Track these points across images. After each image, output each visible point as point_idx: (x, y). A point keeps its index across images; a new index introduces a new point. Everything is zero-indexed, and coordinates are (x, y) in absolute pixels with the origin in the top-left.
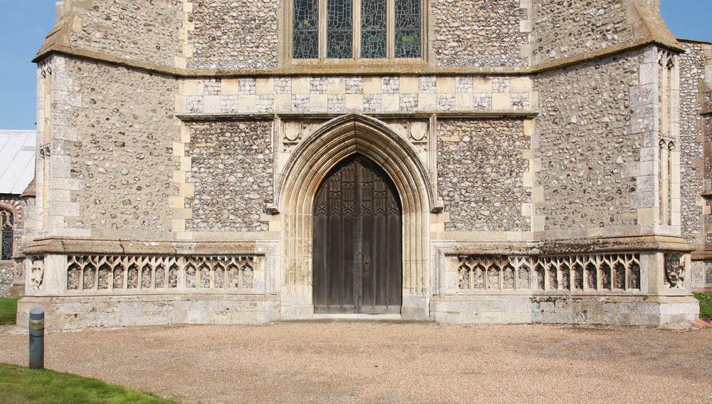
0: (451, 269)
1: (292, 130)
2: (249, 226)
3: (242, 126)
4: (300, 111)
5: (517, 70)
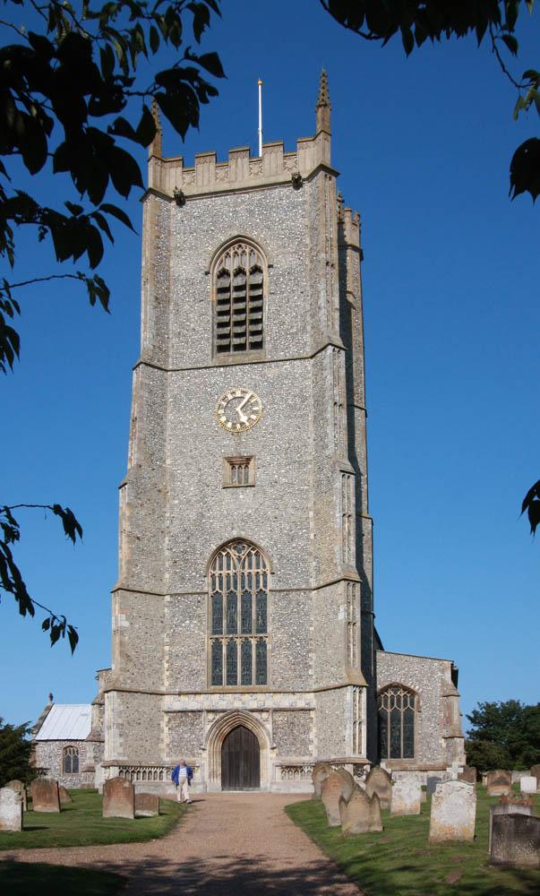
0: (278, 771)
1: (211, 716)
2: (194, 756)
3: (190, 714)
4: (214, 708)
5: (307, 690)
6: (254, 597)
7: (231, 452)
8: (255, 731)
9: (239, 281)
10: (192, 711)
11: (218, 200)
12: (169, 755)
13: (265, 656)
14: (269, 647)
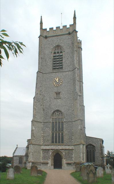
1: (51, 151)
6: (61, 123)
7: (56, 91)
8: (61, 154)
9: (58, 55)
10: (48, 149)
11: (54, 38)
12: (42, 160)
13: (63, 137)
14: (64, 135)
